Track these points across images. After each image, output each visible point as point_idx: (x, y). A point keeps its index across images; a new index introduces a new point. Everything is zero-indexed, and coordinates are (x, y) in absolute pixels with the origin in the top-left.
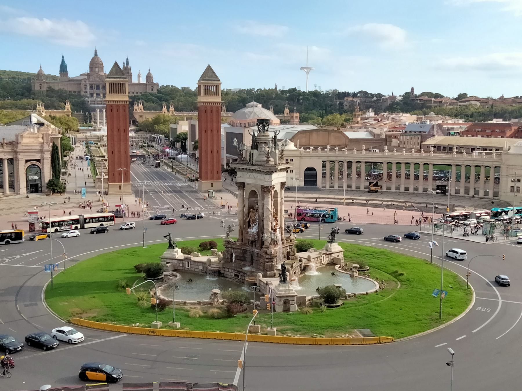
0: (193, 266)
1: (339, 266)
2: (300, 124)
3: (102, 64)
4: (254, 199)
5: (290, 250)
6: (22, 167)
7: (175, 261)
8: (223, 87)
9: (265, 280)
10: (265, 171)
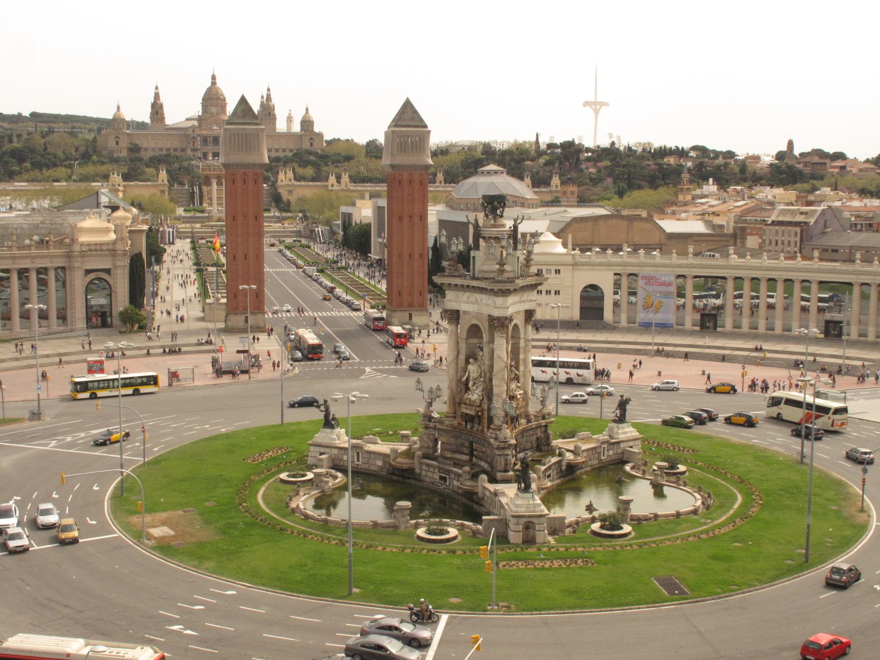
0: (366, 460)
1: (631, 465)
2: (577, 206)
3: (224, 99)
4: (474, 341)
5: (542, 435)
6: (78, 282)
7: (335, 451)
9: (492, 487)
10: (496, 289)
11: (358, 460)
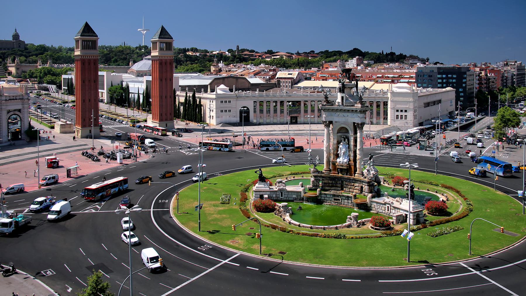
0: (286, 196)
8: (100, 43)
11: (282, 196)
